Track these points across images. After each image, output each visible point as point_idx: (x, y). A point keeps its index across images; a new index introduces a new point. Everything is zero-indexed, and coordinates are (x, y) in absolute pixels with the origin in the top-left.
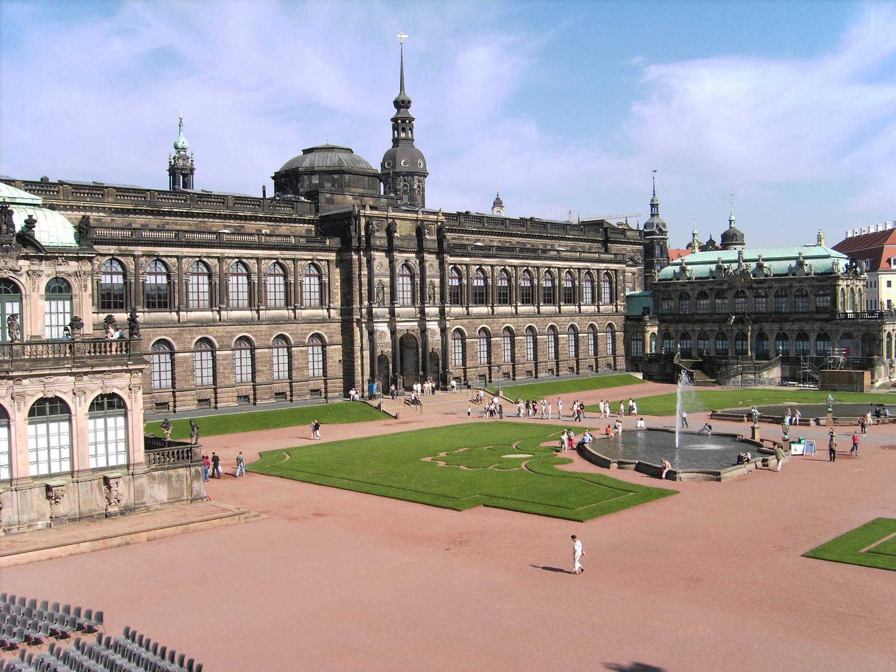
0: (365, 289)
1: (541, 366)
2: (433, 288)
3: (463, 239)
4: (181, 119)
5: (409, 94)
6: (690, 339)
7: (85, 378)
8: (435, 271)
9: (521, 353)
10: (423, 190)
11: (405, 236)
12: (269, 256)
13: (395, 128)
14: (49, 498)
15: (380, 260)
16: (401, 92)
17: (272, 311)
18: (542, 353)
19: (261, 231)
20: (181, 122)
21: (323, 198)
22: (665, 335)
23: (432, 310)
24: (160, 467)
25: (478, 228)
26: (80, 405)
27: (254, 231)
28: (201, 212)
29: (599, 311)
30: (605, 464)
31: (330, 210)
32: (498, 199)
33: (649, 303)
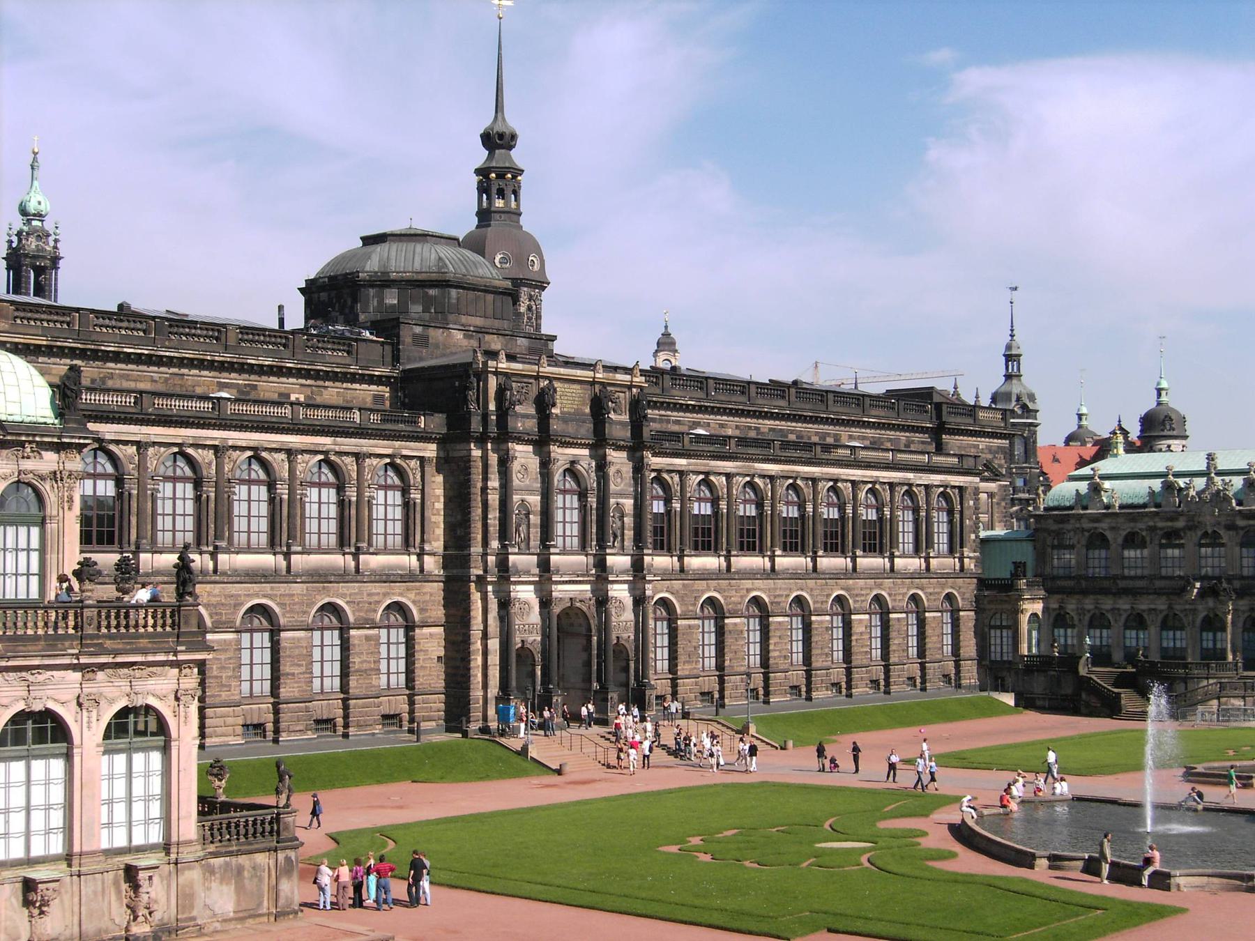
0: (494, 516)
1: (818, 676)
2: (622, 517)
3: (668, 421)
4: (35, 154)
5: (514, 120)
6: (1108, 627)
7: (101, 675)
8: (625, 485)
9: (780, 651)
10: (539, 317)
11: (569, 413)
12: (312, 448)
13: (483, 189)
14: (27, 903)
15: (523, 461)
16: (496, 117)
17: (312, 557)
18: (819, 651)
19: (288, 396)
20: (35, 160)
21: (408, 333)
22: (1056, 619)
23: (619, 561)
24: (223, 850)
25: (699, 400)
26: (89, 727)
27: (275, 397)
28: (176, 355)
29: (928, 568)
30: (1024, 860)
31: (421, 359)
32: (666, 335)
33: (1026, 553)
